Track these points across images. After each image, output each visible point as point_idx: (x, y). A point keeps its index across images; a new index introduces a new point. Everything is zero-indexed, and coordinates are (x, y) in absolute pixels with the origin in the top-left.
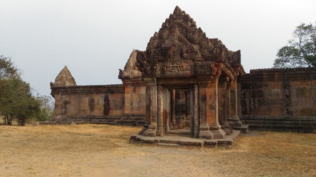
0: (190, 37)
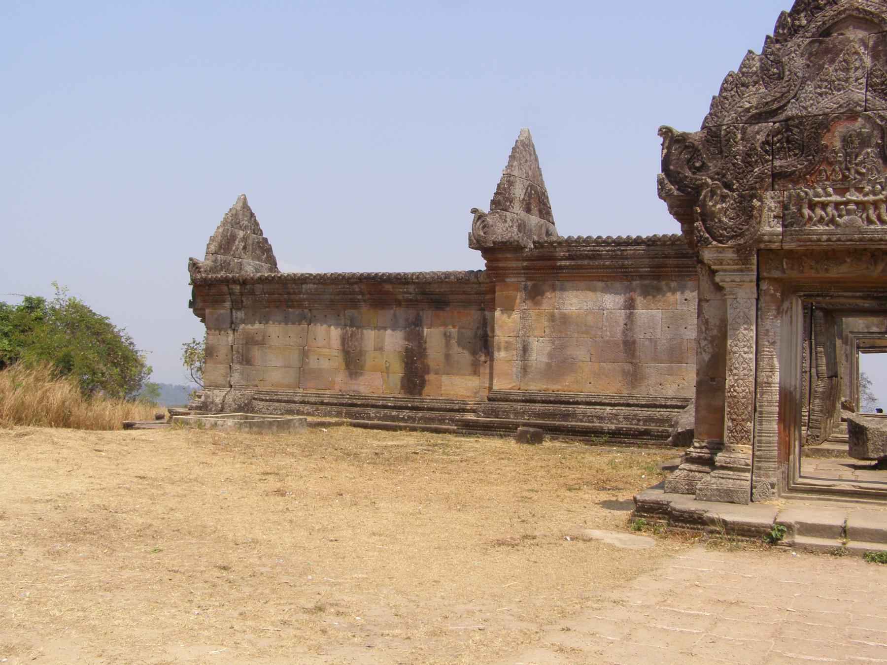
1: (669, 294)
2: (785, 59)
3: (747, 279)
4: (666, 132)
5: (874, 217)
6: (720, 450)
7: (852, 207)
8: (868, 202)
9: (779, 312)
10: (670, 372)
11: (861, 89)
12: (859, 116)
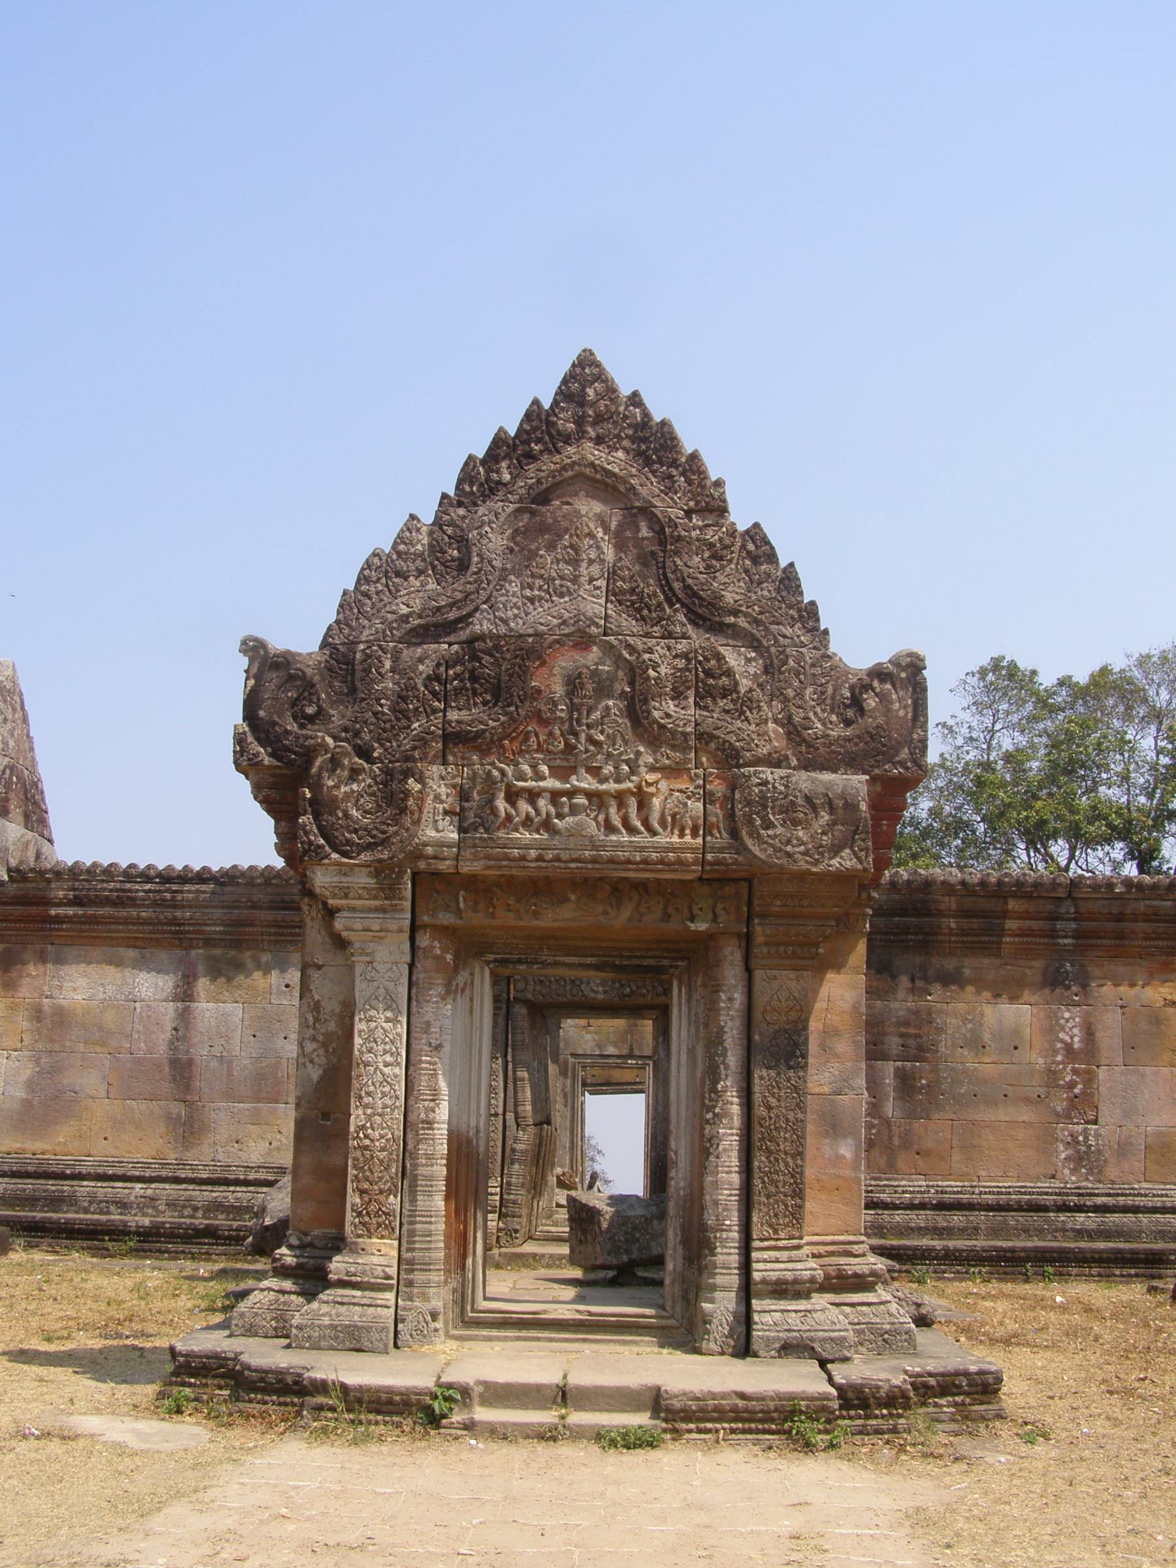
0: (690, 581)
1: (257, 975)
2: (473, 535)
3: (393, 926)
4: (254, 648)
5: (617, 821)
6: (338, 1250)
7: (581, 800)
8: (607, 793)
9: (450, 990)
10: (256, 1119)
11: (598, 597)
12: (595, 643)
